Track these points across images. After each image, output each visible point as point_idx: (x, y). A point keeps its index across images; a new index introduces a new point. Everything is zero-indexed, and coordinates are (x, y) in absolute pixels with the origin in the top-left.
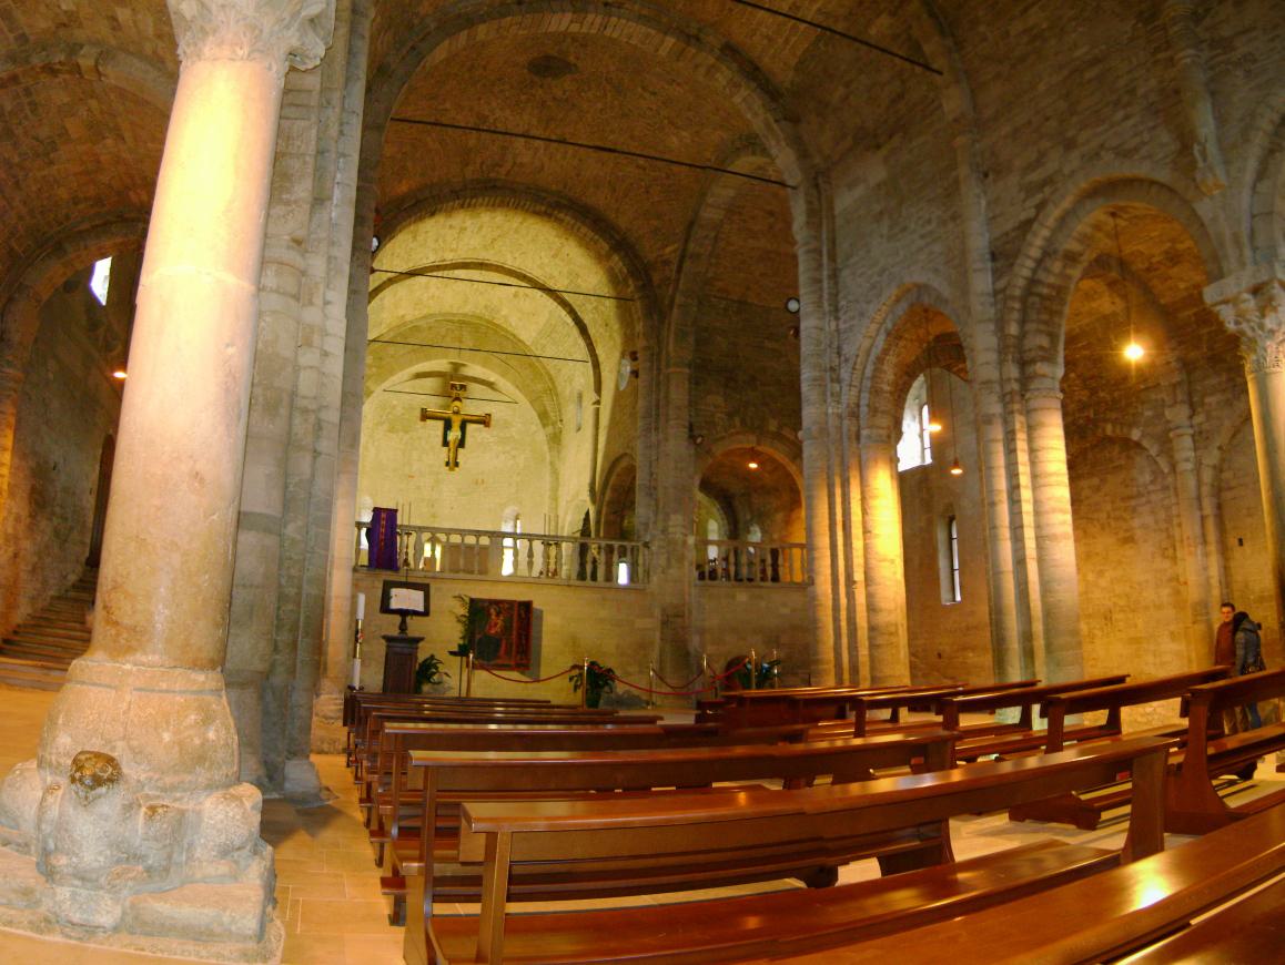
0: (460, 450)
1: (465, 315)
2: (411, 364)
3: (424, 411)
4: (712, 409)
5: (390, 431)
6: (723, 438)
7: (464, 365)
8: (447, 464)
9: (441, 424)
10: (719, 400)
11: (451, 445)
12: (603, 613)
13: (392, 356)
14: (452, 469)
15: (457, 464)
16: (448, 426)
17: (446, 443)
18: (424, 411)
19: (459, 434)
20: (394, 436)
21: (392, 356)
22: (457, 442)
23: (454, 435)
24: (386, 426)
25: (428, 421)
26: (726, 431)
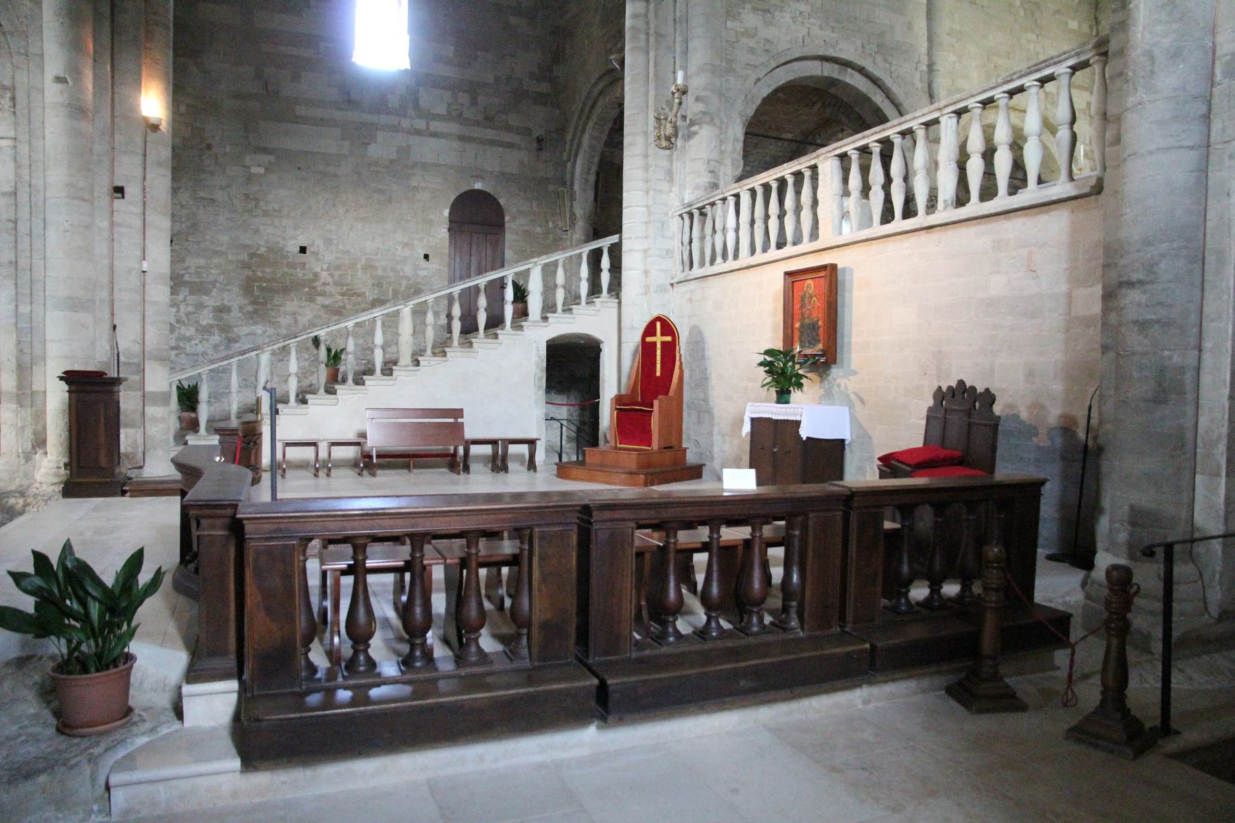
12: (997, 286)
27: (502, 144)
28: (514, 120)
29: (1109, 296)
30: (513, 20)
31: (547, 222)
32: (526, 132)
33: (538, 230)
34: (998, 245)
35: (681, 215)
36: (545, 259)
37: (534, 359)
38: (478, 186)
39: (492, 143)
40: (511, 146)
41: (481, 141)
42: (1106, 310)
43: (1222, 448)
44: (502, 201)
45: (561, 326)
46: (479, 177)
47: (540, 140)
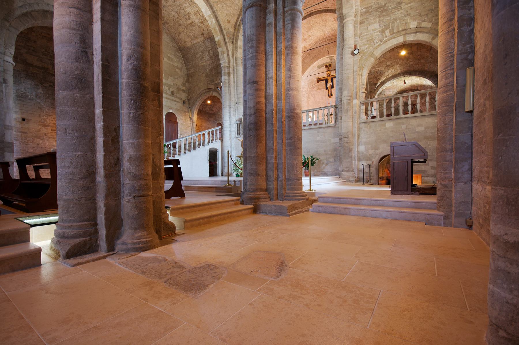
0: (332, 89)
1: (329, 37)
2: (312, 63)
3: (318, 79)
4: (372, 32)
5: (318, 90)
6: (380, 45)
7: (333, 57)
8: (328, 96)
9: (324, 82)
10: (376, 26)
11: (329, 88)
12: (318, 138)
13: (306, 63)
14: (330, 97)
15: (332, 95)
16: (327, 82)
17: (327, 88)
18: (318, 79)
19: (331, 83)
20: (320, 91)
21: (306, 63)
22: (331, 87)
23: (329, 84)
24: (315, 89)
25: (320, 82)
26: (381, 41)
27: (176, 101)
28: (178, 95)
29: (341, 139)
30: (177, 70)
31: (186, 122)
32: (180, 99)
33: (185, 124)
34: (318, 132)
35: (237, 124)
36: (208, 131)
37: (207, 153)
38: (171, 111)
39: (173, 100)
40: (178, 102)
41: (171, 100)
42: (340, 141)
43: (356, 157)
44: (176, 116)
45: (212, 146)
46: (171, 109)
47: (184, 102)
